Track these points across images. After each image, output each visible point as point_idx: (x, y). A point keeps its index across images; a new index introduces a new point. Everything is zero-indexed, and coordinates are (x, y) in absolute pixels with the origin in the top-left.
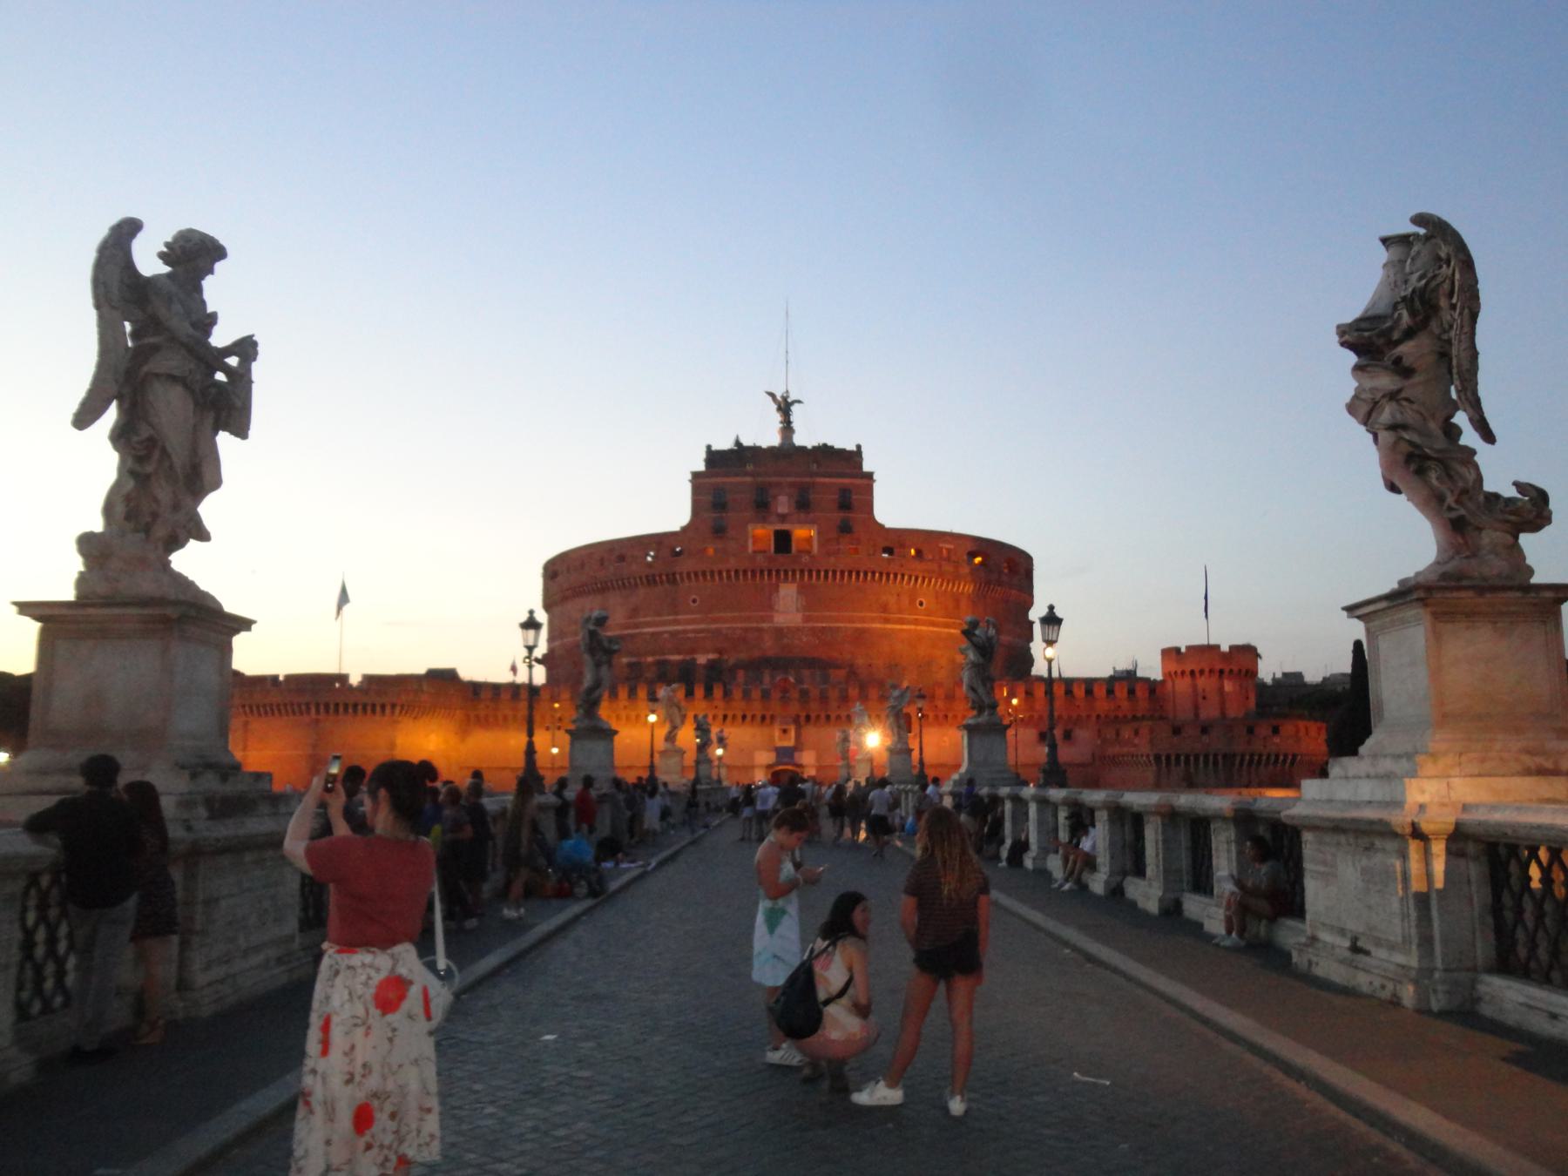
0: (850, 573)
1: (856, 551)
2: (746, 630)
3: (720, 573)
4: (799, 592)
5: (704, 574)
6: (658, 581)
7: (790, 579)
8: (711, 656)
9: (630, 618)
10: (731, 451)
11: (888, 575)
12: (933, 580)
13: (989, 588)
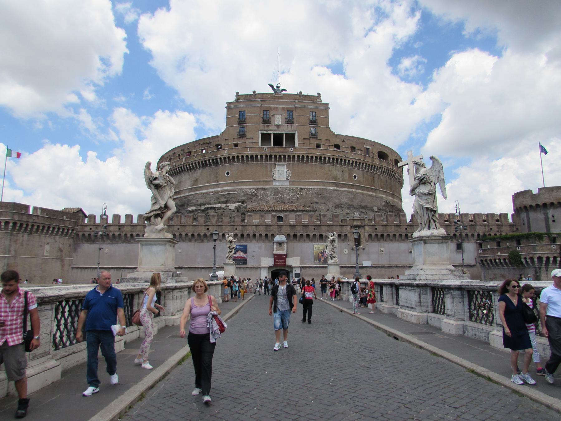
0: (316, 157)
1: (318, 146)
2: (257, 189)
3: (242, 157)
4: (287, 168)
5: (233, 157)
6: (208, 164)
7: (282, 161)
8: (237, 205)
9: (193, 185)
10: (250, 95)
11: (337, 159)
12: (361, 164)
13: (388, 172)
